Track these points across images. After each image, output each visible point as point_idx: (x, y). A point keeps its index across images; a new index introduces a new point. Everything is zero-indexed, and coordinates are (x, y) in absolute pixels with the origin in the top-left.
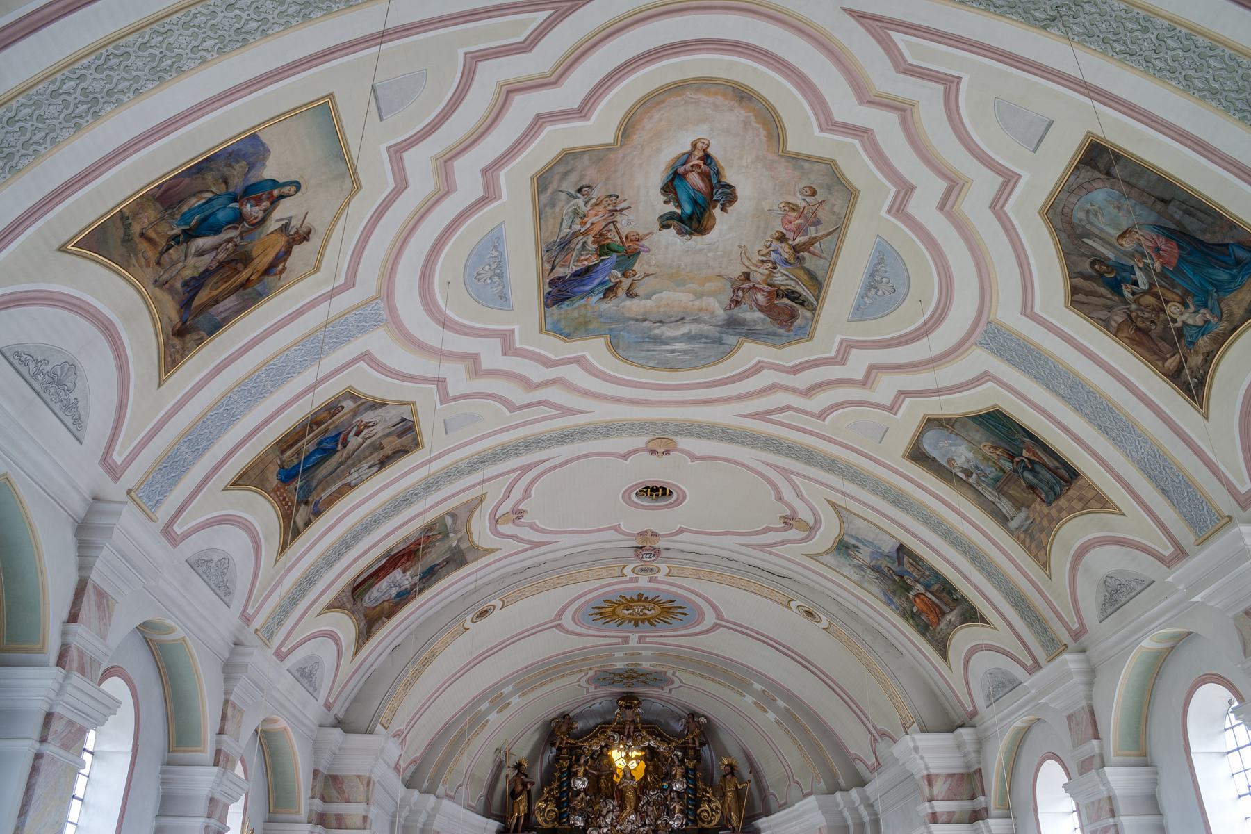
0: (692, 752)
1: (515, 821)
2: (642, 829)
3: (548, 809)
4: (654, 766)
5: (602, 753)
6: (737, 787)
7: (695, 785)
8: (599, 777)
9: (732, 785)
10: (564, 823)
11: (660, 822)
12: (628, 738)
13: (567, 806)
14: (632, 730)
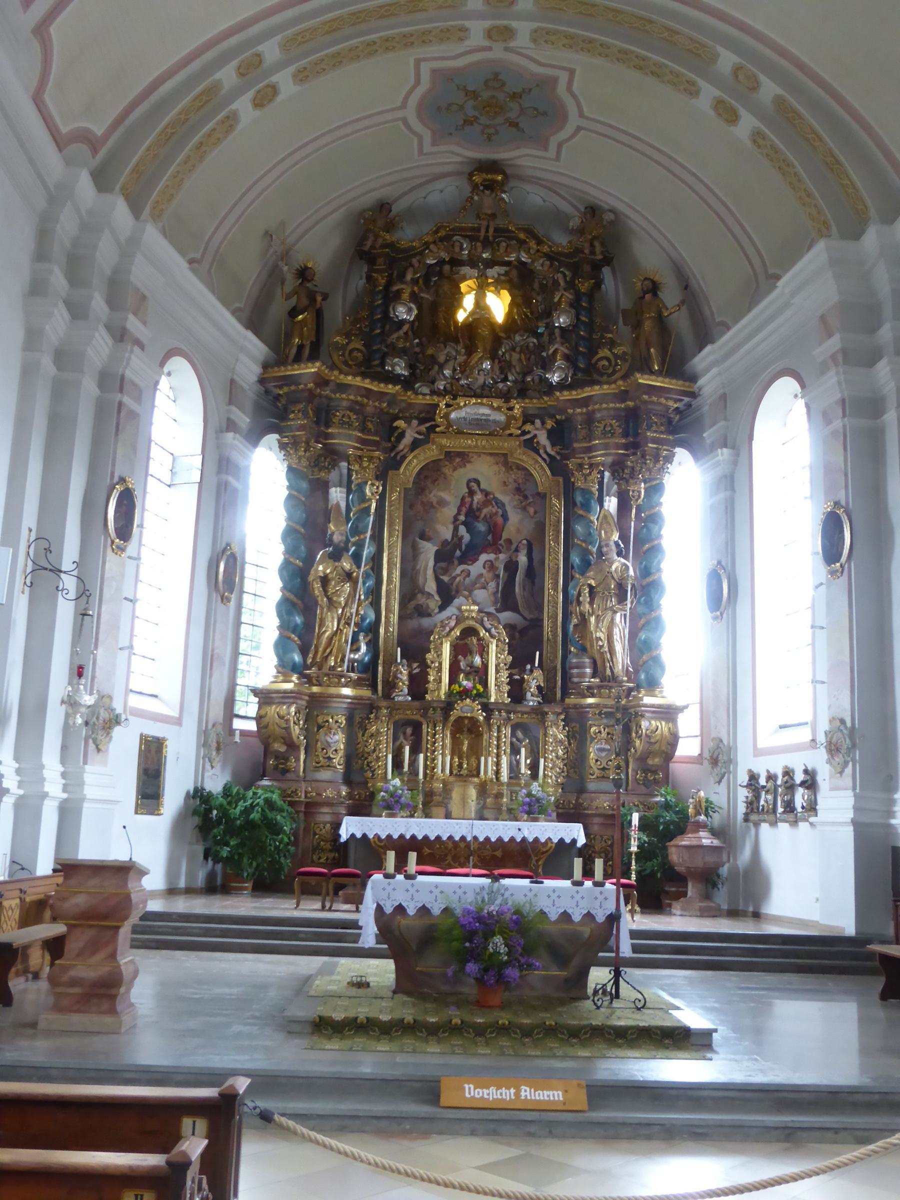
0: (587, 268)
1: (294, 350)
2: (501, 385)
3: (351, 346)
5: (440, 274)
10: (376, 366)
14: (491, 230)
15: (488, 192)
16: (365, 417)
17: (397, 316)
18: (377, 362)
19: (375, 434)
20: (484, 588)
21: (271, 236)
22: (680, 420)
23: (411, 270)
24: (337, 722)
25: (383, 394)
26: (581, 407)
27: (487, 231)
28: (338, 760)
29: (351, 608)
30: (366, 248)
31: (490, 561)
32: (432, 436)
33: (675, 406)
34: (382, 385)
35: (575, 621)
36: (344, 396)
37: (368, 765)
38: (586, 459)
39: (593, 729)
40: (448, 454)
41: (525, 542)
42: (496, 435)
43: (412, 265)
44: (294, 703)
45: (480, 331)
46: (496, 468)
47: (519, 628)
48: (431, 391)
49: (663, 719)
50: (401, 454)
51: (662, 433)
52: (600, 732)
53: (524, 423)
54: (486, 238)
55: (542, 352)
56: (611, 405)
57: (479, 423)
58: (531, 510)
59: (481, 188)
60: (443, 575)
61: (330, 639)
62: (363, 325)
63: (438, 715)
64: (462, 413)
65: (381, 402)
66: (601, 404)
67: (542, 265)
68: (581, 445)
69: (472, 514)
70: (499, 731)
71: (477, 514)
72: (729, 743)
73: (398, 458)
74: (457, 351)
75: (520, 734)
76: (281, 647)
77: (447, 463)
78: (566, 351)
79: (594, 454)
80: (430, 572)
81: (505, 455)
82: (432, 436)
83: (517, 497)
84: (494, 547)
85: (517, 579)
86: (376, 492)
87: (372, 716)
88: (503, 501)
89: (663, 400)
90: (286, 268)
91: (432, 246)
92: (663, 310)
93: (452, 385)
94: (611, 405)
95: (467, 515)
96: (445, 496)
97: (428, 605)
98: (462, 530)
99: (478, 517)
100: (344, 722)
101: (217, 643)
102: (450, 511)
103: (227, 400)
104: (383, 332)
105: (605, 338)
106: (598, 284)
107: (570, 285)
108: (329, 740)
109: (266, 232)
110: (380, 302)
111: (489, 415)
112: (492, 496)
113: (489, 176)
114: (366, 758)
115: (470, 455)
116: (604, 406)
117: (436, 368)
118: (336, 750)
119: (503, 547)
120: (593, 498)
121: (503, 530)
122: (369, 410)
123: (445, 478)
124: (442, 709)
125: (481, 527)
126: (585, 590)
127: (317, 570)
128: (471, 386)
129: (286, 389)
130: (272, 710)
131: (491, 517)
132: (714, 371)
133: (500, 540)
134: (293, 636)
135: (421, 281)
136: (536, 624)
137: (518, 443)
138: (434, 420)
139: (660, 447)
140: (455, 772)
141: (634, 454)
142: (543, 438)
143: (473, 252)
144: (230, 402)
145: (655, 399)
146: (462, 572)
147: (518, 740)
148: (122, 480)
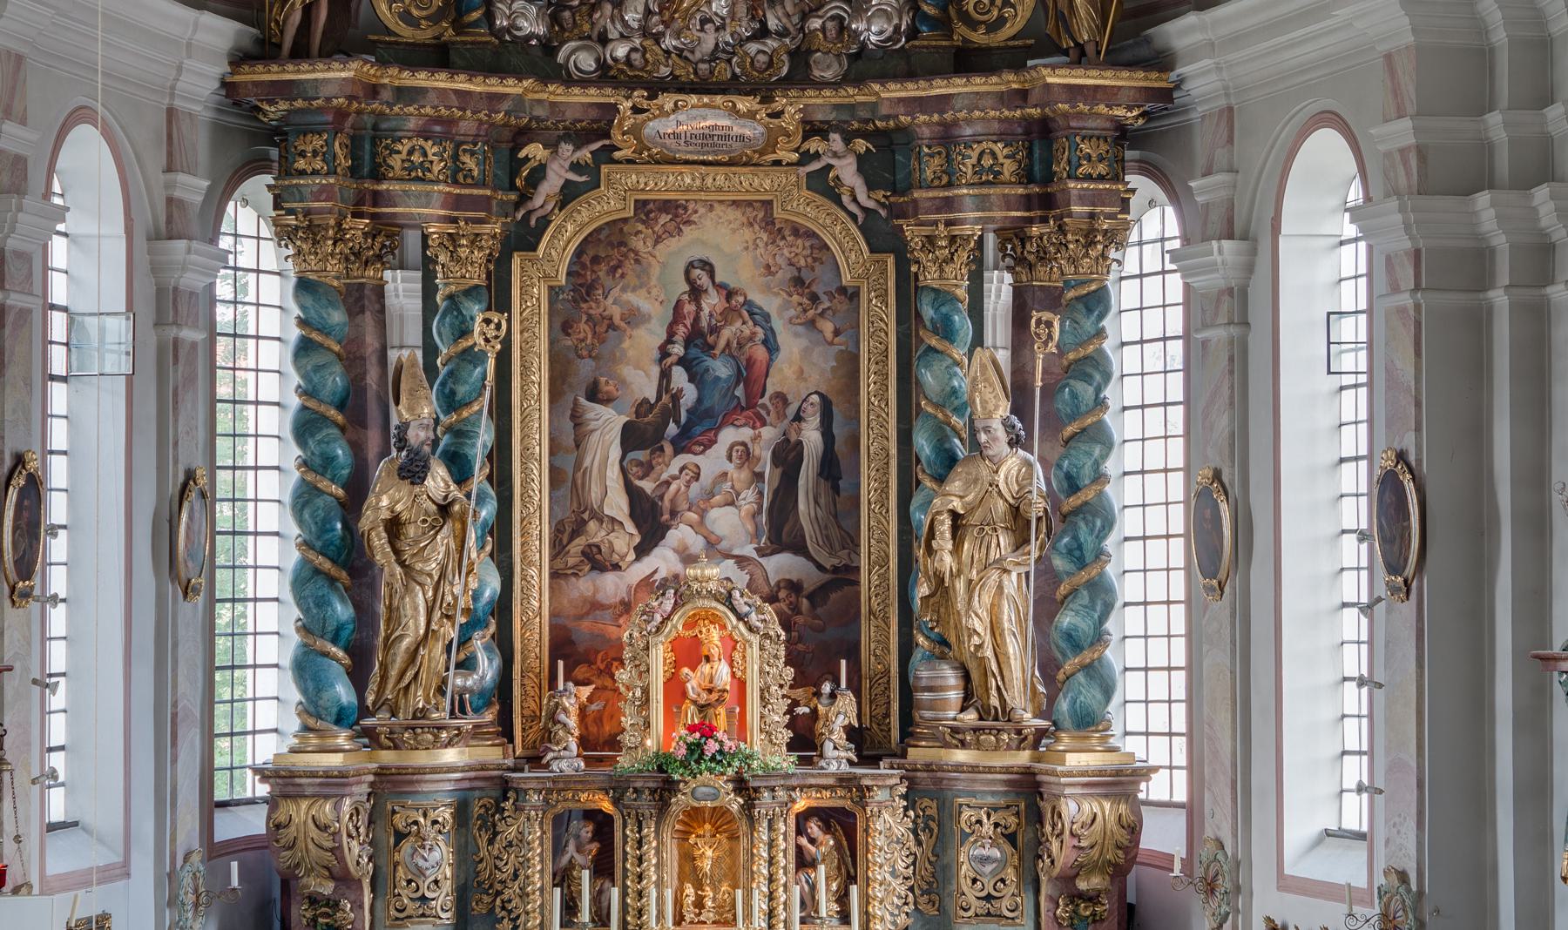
1: (297, 17)
2: (753, 48)
10: (475, 24)
11: (816, 23)
19: (484, 185)
20: (732, 504)
24: (435, 822)
28: (443, 898)
29: (452, 584)
31: (744, 444)
32: (605, 169)
34: (494, 80)
35: (923, 590)
37: (503, 908)
38: (942, 227)
39: (966, 814)
40: (641, 205)
41: (815, 398)
42: (745, 165)
44: (343, 796)
46: (747, 234)
47: (809, 587)
48: (598, 60)
49: (1106, 796)
50: (540, 213)
51: (1101, 178)
52: (979, 822)
53: (805, 138)
58: (828, 327)
60: (641, 478)
61: (413, 655)
63: (646, 804)
64: (667, 126)
66: (971, 111)
68: (931, 194)
69: (700, 340)
70: (771, 828)
71: (711, 339)
72: (1235, 855)
73: (533, 222)
75: (814, 828)
76: (306, 668)
77: (641, 227)
80: (613, 473)
81: (768, 204)
82: (605, 169)
83: (796, 298)
84: (749, 413)
85: (801, 482)
86: (496, 337)
87: (508, 805)
88: (766, 309)
89: (1102, 109)
95: (688, 343)
96: (639, 300)
97: (610, 543)
98: (679, 377)
99: (713, 348)
100: (451, 821)
101: (181, 689)
102: (649, 338)
103: (163, 160)
108: (421, 863)
111: (731, 128)
112: (741, 299)
114: (499, 893)
115: (691, 206)
118: (436, 882)
119: (768, 414)
120: (959, 311)
121: (767, 376)
123: (637, 261)
124: (653, 792)
125: (721, 369)
126: (942, 523)
127: (377, 509)
128: (686, 53)
130: (299, 812)
131: (740, 346)
132: (1206, 63)
133: (762, 396)
134: (334, 649)
136: (845, 576)
138: (608, 136)
140: (688, 917)
141: (1044, 220)
142: (847, 172)
144: (169, 169)
146: (682, 470)
147: (812, 841)
148: (19, 460)
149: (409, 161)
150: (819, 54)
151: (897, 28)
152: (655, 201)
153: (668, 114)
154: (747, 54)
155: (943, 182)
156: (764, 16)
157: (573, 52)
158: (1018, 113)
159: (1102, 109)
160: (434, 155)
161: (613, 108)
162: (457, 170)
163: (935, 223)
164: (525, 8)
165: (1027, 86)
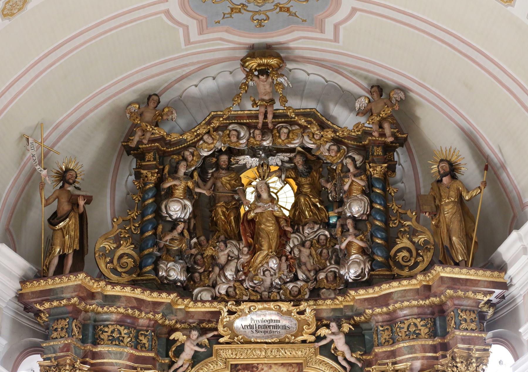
0: (378, 151)
1: (56, 261)
2: (290, 286)
4: (312, 185)
5: (217, 166)
6: (461, 197)
7: (386, 207)
8: (213, 201)
9: (452, 193)
10: (149, 272)
11: (322, 276)
12: (263, 134)
13: (156, 244)
14: (270, 116)
15: (262, 78)
16: (138, 331)
17: (170, 216)
18: (149, 268)
19: (151, 350)
21: (28, 139)
22: (495, 313)
23: (183, 164)
25: (156, 304)
26: (381, 306)
27: (265, 117)
30: (133, 145)
32: (216, 347)
33: (486, 299)
34: (155, 294)
36: (112, 309)
38: (390, 365)
43: (185, 159)
45: (263, 226)
54: (265, 124)
55: (335, 244)
56: (415, 303)
57: (266, 328)
59: (256, 73)
62: (133, 227)
65: (156, 313)
67: (329, 150)
74: (239, 250)
78: (361, 244)
79: (398, 359)
89: (470, 294)
90: (44, 172)
91: (205, 137)
92: (464, 194)
93: (235, 288)
94: (415, 303)
104: (155, 234)
105: (403, 226)
106: (392, 168)
107: (361, 170)
109: (22, 136)
110: (151, 201)
113: (265, 61)
115: (260, 367)
116: (406, 304)
117: (217, 270)
122: (141, 321)
129: (47, 305)
135: (196, 174)
137: (313, 350)
138: (216, 329)
139: (472, 347)
141: (444, 356)
143: (252, 140)
145: (460, 293)
149: (112, 336)
150: (324, 290)
151: (363, 270)
152: (241, 364)
153: (246, 315)
154: (287, 288)
155: (390, 343)
156: (296, 272)
157: (200, 292)
158: (427, 302)
159: (470, 294)
160: (125, 334)
161: (218, 314)
162: (138, 343)
163: (387, 364)
164: (174, 266)
165: (431, 284)
